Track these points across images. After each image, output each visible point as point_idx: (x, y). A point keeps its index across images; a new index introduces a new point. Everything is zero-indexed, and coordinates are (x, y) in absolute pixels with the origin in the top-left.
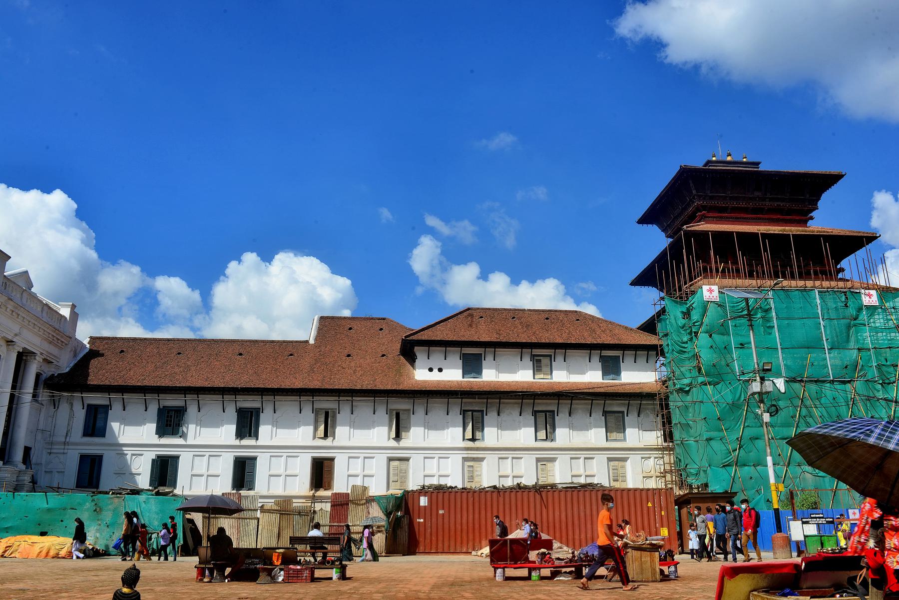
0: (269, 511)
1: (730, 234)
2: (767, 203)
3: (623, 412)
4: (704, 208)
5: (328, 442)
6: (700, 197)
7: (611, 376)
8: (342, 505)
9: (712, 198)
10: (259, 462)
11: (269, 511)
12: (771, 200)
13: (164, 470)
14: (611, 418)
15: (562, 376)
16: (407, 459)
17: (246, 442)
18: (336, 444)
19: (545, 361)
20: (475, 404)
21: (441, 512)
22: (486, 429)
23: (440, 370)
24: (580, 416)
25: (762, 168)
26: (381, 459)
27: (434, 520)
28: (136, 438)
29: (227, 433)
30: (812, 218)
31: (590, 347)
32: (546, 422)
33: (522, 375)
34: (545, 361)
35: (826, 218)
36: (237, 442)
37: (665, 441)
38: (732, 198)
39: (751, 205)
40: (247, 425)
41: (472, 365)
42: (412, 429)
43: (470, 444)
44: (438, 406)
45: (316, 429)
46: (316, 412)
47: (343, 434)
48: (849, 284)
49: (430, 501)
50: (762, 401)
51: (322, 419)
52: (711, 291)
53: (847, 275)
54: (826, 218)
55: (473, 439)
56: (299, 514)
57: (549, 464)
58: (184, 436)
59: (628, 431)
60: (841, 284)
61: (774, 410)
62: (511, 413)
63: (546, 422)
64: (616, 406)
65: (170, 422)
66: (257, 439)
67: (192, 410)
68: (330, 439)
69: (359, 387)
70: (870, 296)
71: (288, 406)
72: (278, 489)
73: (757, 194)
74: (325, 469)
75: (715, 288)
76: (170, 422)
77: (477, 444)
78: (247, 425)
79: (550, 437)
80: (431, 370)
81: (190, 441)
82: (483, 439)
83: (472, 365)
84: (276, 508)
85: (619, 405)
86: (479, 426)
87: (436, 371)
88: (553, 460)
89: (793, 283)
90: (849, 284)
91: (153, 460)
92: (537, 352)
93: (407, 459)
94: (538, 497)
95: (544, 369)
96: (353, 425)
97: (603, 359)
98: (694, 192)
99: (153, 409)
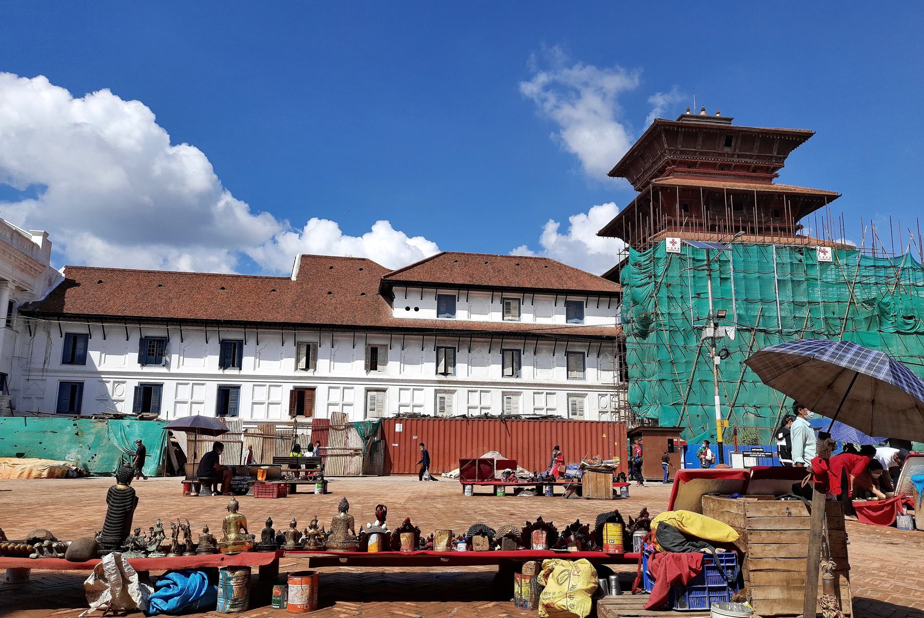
0: (253, 435)
1: (696, 189)
2: (736, 160)
3: (584, 353)
4: (674, 162)
5: (309, 373)
6: (670, 151)
7: (575, 320)
8: (322, 430)
9: (682, 152)
10: (243, 391)
11: (253, 435)
12: (739, 156)
13: (148, 398)
14: (572, 359)
15: (530, 317)
16: (384, 391)
17: (228, 372)
18: (316, 375)
19: (514, 304)
20: (449, 342)
21: (415, 437)
22: (458, 365)
23: (417, 309)
24: (544, 356)
25: (733, 124)
26: (360, 389)
27: (408, 445)
28: (116, 367)
29: (210, 363)
30: (777, 176)
31: (556, 292)
32: (513, 361)
33: (491, 316)
34: (514, 304)
35: (791, 177)
36: (221, 372)
37: (621, 380)
38: (701, 153)
39: (719, 161)
40: (231, 356)
41: (446, 306)
42: (390, 363)
43: (443, 378)
44: (414, 341)
45: (298, 361)
46: (298, 345)
47: (323, 366)
48: (806, 241)
49: (405, 428)
50: (714, 345)
51: (304, 351)
52: (673, 243)
53: (806, 232)
54: (791, 177)
55: (445, 374)
56: (282, 437)
57: (514, 398)
58: (167, 365)
59: (588, 370)
60: (798, 241)
61: (726, 354)
62: (480, 352)
63: (513, 361)
64: (578, 347)
65: (153, 352)
66: (241, 369)
67: (175, 341)
68: (311, 370)
69: (339, 323)
70: (825, 252)
71: (271, 340)
72: (260, 415)
73: (727, 150)
74: (307, 398)
75: (678, 240)
76: (153, 352)
77: (449, 378)
78: (231, 356)
79: (516, 373)
80: (408, 309)
81: (174, 369)
82: (455, 374)
83: (446, 306)
84: (260, 432)
85: (580, 346)
86: (451, 362)
87: (412, 310)
88: (518, 394)
89: (753, 238)
90: (806, 241)
91: (136, 388)
92: (507, 295)
93: (384, 391)
94: (503, 426)
95: (513, 311)
96: (333, 358)
97: (567, 304)
98: (666, 146)
99: (135, 339)
